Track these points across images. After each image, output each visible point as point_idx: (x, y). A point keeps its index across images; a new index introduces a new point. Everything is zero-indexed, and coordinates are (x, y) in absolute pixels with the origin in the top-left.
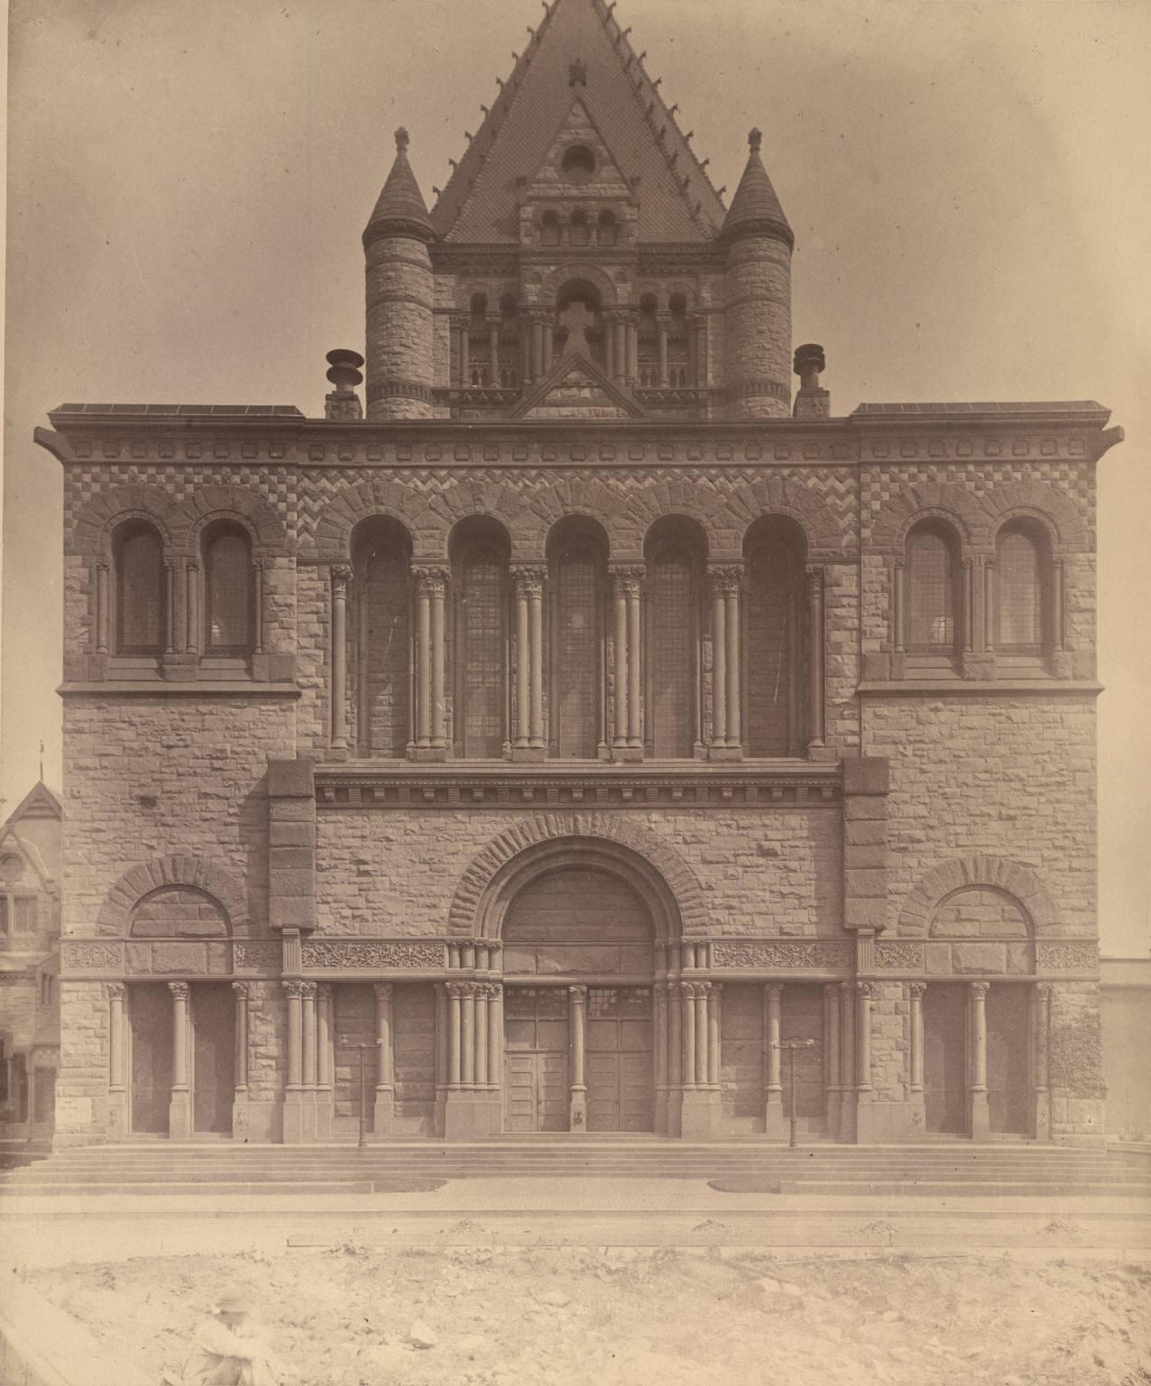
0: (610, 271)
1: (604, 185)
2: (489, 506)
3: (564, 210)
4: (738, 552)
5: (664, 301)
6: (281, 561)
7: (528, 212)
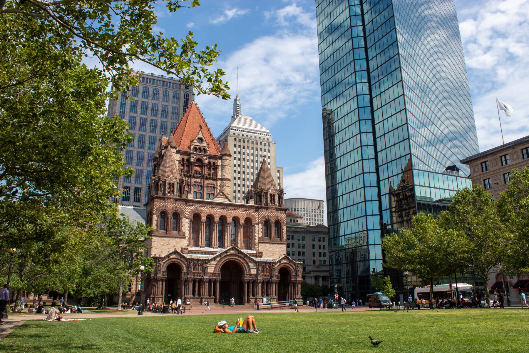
0: (205, 158)
1: (204, 144)
2: (212, 213)
3: (198, 147)
5: (212, 163)
7: (192, 147)
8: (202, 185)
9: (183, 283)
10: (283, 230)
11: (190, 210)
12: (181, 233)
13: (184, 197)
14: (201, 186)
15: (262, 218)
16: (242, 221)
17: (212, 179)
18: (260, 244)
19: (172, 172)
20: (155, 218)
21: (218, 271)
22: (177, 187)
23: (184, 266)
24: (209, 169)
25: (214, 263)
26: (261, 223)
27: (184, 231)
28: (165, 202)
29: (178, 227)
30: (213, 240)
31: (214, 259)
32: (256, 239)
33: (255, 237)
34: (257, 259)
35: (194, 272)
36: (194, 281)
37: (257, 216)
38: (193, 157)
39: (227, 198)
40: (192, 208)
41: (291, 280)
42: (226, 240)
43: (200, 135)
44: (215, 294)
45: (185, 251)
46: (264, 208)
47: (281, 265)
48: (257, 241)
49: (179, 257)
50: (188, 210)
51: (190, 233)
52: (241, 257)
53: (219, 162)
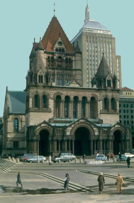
0: (64, 55)
1: (63, 46)
2: (69, 95)
3: (58, 48)
4: (90, 100)
5: (68, 59)
6: (50, 99)
8: (63, 74)
9: (50, 143)
10: (116, 104)
11: (54, 93)
12: (48, 109)
13: (50, 84)
14: (62, 75)
15: (102, 97)
16: (89, 99)
17: (70, 70)
18: (101, 115)
19: (41, 68)
20: (31, 100)
21: (73, 134)
22: (45, 80)
23: (50, 131)
24: (67, 62)
25: (71, 128)
26: (102, 100)
27: (50, 108)
28: (37, 89)
29: (46, 105)
30: (70, 113)
31: (70, 126)
32: (98, 111)
33: (98, 110)
34: (99, 125)
35: (57, 135)
36: (58, 141)
37: (100, 96)
38: (55, 55)
39: (78, 83)
40: (55, 92)
41: (122, 139)
42: (79, 113)
43: (60, 40)
44: (71, 150)
45: (52, 121)
46: (104, 90)
47: (115, 129)
48: (99, 113)
49: (47, 125)
50: (52, 93)
51: (54, 109)
52: (88, 124)
53: (73, 58)
